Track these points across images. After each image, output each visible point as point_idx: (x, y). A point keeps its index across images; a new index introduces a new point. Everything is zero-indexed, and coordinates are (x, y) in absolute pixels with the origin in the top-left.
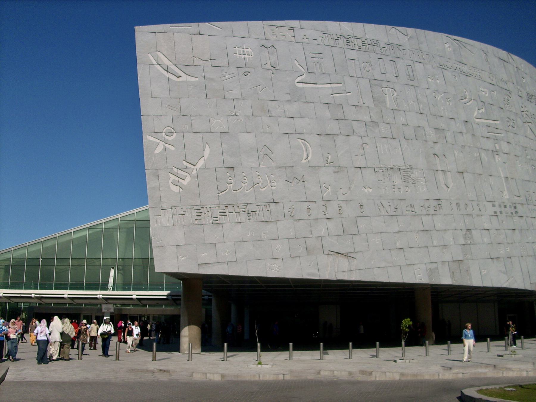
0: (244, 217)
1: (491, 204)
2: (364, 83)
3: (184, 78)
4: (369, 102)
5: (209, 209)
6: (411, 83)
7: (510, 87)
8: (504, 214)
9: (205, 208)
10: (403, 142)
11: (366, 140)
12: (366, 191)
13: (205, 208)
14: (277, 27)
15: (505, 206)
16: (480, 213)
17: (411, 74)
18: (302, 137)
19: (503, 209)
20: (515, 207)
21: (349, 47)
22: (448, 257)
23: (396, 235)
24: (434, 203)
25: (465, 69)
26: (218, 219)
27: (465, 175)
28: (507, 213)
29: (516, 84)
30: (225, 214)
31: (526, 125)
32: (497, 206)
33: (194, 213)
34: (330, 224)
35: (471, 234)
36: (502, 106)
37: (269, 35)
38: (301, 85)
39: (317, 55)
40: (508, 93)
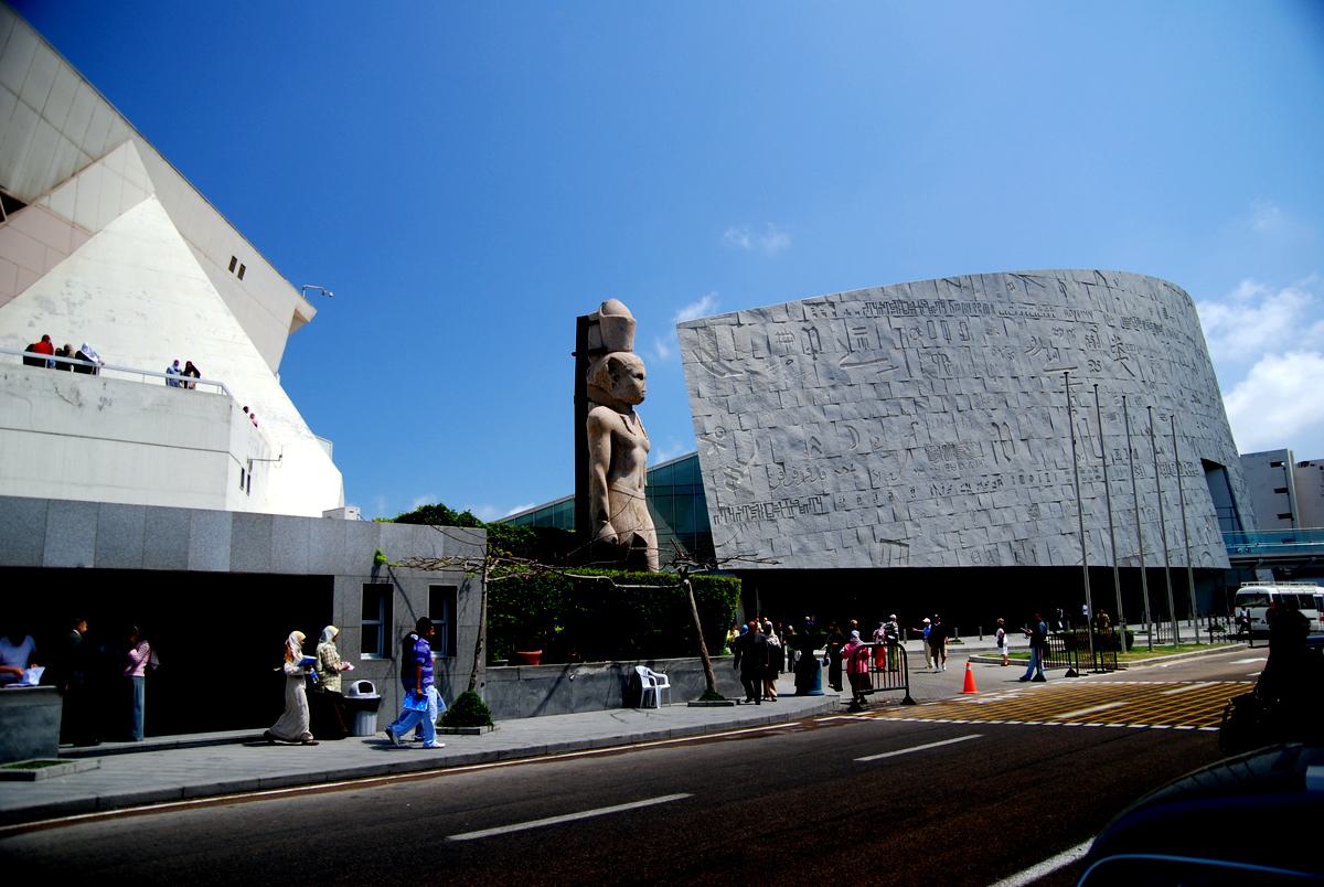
0: (796, 511)
2: (912, 353)
3: (728, 375)
4: (917, 375)
7: (1097, 318)
11: (915, 418)
14: (817, 305)
16: (1049, 484)
17: (965, 333)
18: (848, 423)
20: (1097, 471)
22: (1007, 537)
24: (994, 479)
25: (1034, 311)
31: (1118, 363)
33: (749, 512)
34: (879, 510)
35: (1037, 509)
36: (1083, 346)
37: (809, 315)
38: (846, 368)
40: (1092, 327)
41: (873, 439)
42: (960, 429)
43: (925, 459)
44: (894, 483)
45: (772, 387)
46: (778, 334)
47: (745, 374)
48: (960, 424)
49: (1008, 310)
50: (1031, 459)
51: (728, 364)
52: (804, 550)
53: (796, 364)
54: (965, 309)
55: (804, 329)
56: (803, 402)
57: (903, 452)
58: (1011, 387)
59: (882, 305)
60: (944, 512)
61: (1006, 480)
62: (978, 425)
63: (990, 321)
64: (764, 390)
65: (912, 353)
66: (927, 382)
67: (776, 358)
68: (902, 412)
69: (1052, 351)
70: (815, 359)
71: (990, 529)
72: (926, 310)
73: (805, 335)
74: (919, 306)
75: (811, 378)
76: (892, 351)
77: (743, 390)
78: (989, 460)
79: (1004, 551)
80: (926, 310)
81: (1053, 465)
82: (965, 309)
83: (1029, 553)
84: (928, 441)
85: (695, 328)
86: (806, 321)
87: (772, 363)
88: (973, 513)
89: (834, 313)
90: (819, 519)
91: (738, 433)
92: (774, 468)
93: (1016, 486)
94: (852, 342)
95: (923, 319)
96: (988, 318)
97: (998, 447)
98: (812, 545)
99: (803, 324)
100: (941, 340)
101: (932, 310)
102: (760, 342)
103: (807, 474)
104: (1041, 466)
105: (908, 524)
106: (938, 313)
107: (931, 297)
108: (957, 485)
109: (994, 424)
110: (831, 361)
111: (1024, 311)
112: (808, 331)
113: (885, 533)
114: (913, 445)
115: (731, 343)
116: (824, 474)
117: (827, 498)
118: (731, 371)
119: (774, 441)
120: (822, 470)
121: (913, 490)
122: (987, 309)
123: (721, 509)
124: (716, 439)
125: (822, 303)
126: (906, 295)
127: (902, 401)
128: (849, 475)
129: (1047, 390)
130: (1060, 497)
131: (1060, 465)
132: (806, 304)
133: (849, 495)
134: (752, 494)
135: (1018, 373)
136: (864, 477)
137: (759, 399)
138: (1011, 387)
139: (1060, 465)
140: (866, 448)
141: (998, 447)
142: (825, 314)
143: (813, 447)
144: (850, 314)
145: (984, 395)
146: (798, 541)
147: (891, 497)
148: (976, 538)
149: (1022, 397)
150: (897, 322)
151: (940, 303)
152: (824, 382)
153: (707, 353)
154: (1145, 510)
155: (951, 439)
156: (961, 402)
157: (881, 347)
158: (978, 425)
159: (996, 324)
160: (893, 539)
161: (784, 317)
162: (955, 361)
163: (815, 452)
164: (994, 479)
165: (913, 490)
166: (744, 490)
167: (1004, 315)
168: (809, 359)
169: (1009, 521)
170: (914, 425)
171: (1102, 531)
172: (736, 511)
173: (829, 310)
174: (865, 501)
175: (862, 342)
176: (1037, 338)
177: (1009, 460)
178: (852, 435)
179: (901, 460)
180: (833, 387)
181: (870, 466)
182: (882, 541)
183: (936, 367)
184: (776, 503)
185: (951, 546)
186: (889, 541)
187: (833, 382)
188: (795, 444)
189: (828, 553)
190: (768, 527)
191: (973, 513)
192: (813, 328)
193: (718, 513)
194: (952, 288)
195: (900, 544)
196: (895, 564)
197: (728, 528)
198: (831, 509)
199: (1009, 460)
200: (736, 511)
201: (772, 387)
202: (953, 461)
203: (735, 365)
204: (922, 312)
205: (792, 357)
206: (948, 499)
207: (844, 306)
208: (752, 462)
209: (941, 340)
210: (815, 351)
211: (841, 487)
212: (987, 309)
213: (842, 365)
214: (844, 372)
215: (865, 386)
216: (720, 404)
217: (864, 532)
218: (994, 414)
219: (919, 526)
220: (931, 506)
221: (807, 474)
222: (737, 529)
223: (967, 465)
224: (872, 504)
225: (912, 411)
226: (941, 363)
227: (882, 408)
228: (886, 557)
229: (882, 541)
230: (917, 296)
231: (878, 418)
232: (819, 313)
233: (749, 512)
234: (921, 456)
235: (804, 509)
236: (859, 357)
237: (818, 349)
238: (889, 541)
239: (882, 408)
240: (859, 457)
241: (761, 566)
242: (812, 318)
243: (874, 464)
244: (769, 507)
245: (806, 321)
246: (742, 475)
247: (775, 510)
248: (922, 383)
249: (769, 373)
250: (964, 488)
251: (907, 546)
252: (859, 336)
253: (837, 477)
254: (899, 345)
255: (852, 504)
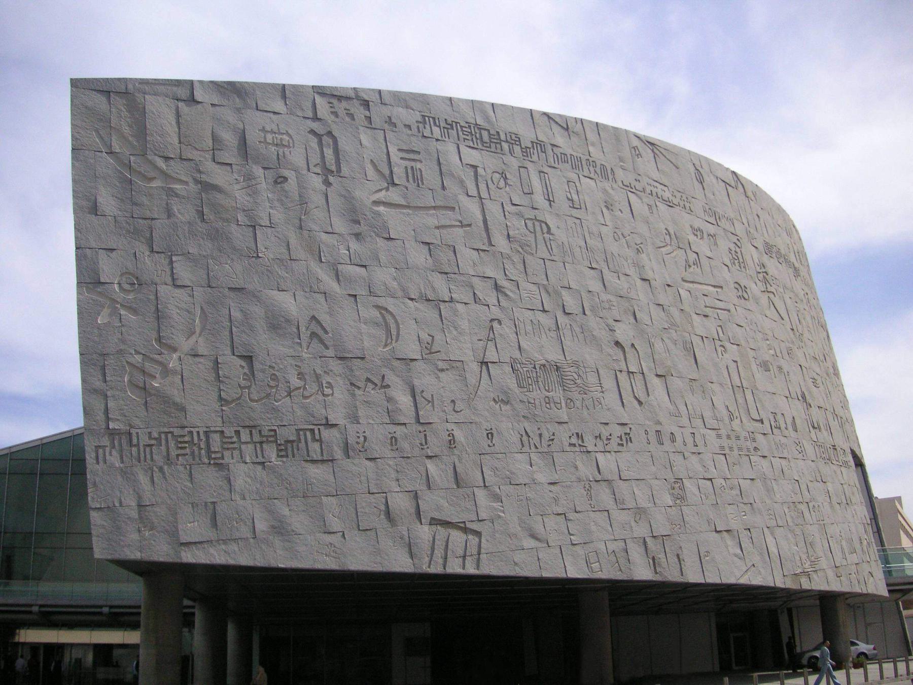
0: (271, 453)
1: (713, 433)
4: (501, 243)
5: (202, 437)
6: (575, 213)
7: (739, 229)
8: (736, 452)
9: (195, 434)
10: (562, 319)
11: (495, 312)
12: (497, 406)
13: (195, 434)
14: (340, 98)
15: (738, 438)
16: (695, 450)
17: (575, 197)
18: (381, 302)
19: (733, 442)
20: (754, 440)
21: (467, 143)
22: (641, 530)
23: (552, 488)
25: (667, 195)
26: (219, 455)
27: (669, 378)
28: (740, 449)
29: (746, 224)
30: (232, 446)
32: (724, 437)
33: (172, 444)
35: (682, 488)
38: (381, 209)
39: (412, 156)
40: (734, 239)
41: (425, 336)
42: (567, 342)
43: (512, 383)
44: (460, 418)
45: (241, 217)
46: (263, 130)
47: (193, 187)
48: (568, 333)
49: (634, 183)
50: (671, 408)
51: (161, 163)
52: (280, 529)
53: (292, 184)
54: (577, 164)
55: (312, 132)
56: (299, 252)
57: (475, 367)
58: (641, 293)
59: (450, 125)
60: (542, 478)
61: (638, 436)
62: (594, 340)
63: (611, 191)
64: (227, 221)
65: (493, 209)
66: (516, 258)
67: (258, 171)
68: (476, 299)
69: (692, 257)
70: (328, 184)
71: (615, 513)
72: (517, 149)
73: (314, 143)
74: (507, 141)
75: (319, 214)
76: (463, 198)
77: (184, 213)
78: (611, 398)
79: (636, 553)
80: (517, 149)
81: (699, 422)
82: (577, 164)
83: (673, 560)
84: (517, 355)
85: (107, 93)
86: (316, 118)
87: (249, 177)
88: (589, 486)
89: (369, 118)
90: (315, 472)
91: (165, 290)
92: (234, 366)
93: (652, 448)
94: (395, 170)
95: (514, 163)
96: (607, 185)
97: (623, 377)
98: (298, 521)
99: (315, 126)
100: (539, 199)
101: (526, 152)
102: (228, 137)
103: (295, 382)
104: (685, 421)
105: (481, 494)
106: (535, 158)
107: (527, 135)
108: (563, 435)
109: (617, 343)
110: (358, 194)
111: (654, 190)
112: (319, 136)
113: (439, 508)
114: (491, 355)
115: (171, 128)
116: (330, 386)
117: (334, 432)
118: (166, 176)
119: (237, 314)
120: (325, 379)
121: (490, 435)
122: (605, 173)
123: (112, 433)
124: (119, 295)
125: (348, 98)
126: (487, 118)
127: (475, 281)
128: (376, 395)
129: (686, 308)
130: (713, 473)
131: (711, 423)
132: (318, 93)
133: (375, 430)
134: (183, 409)
135: (650, 275)
136: (404, 400)
137: (216, 236)
138: (641, 293)
139: (711, 423)
140: (412, 349)
141: (623, 377)
142: (352, 116)
143: (314, 335)
144: (395, 125)
145: (604, 297)
146: (271, 512)
147: (452, 442)
148: (594, 528)
149: (656, 312)
150: (472, 156)
151: (538, 144)
152: (340, 225)
153: (123, 137)
154: (811, 505)
155: (554, 355)
156: (569, 300)
157: (443, 188)
158: (594, 340)
159: (619, 196)
160: (455, 520)
161: (279, 106)
162: (560, 235)
163: (315, 344)
164: (618, 431)
165: (490, 435)
166: (166, 400)
167: (628, 187)
168: (316, 182)
169: (644, 503)
170: (495, 324)
171: (766, 530)
172: (144, 440)
173: (360, 113)
174: (405, 445)
175: (416, 177)
176: (672, 232)
177: (640, 403)
178: (389, 328)
179: (472, 380)
180: (357, 236)
181: (416, 382)
182: (434, 522)
183: (531, 238)
184: (229, 432)
185: (553, 539)
186: (446, 524)
187: (356, 229)
188: (277, 324)
189: (328, 538)
190: (209, 477)
191: (589, 486)
192: (330, 133)
193: (105, 441)
194: (556, 128)
195: (465, 530)
196: (455, 567)
197: (123, 473)
198: (338, 454)
199: (640, 403)
200: (144, 440)
201: (241, 217)
202: (557, 394)
203: (177, 169)
204: (511, 152)
205: (286, 173)
206: (548, 456)
207: (386, 111)
208: (185, 345)
209: (539, 199)
210: (327, 171)
211: (361, 413)
212: (605, 173)
213: (377, 203)
214: (378, 214)
215: (413, 243)
216: (135, 233)
217: (401, 503)
218: (617, 326)
219: (497, 498)
220: (519, 464)
221: (295, 382)
222: (143, 479)
223: (578, 404)
224: (417, 451)
225: (492, 300)
226: (539, 234)
227: (441, 286)
228: (439, 553)
229: (434, 522)
230: (505, 126)
231: (435, 302)
232: (342, 113)
233: (172, 444)
234: (504, 376)
235: (286, 449)
236: (405, 197)
237: (333, 168)
238: (446, 524)
239: (441, 286)
240: (396, 363)
241: (189, 557)
242: (330, 118)
243: (425, 380)
244: (216, 437)
245: (316, 118)
246: (166, 371)
247: (227, 444)
248: (509, 258)
249: (240, 196)
250: (574, 440)
251: (478, 534)
252: (409, 164)
253: (353, 395)
254: (473, 191)
255: (378, 448)
